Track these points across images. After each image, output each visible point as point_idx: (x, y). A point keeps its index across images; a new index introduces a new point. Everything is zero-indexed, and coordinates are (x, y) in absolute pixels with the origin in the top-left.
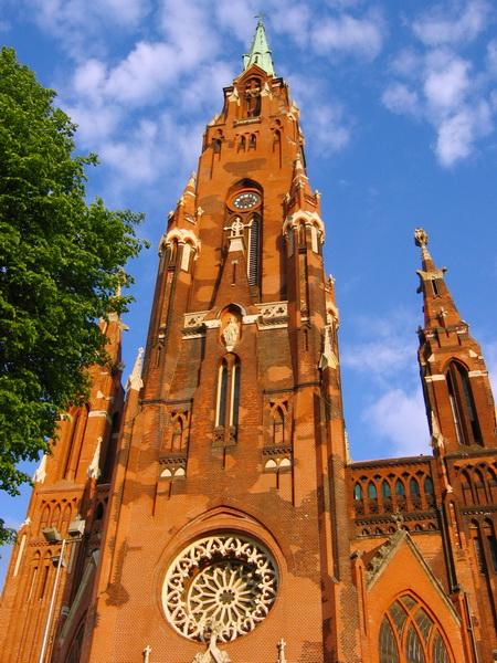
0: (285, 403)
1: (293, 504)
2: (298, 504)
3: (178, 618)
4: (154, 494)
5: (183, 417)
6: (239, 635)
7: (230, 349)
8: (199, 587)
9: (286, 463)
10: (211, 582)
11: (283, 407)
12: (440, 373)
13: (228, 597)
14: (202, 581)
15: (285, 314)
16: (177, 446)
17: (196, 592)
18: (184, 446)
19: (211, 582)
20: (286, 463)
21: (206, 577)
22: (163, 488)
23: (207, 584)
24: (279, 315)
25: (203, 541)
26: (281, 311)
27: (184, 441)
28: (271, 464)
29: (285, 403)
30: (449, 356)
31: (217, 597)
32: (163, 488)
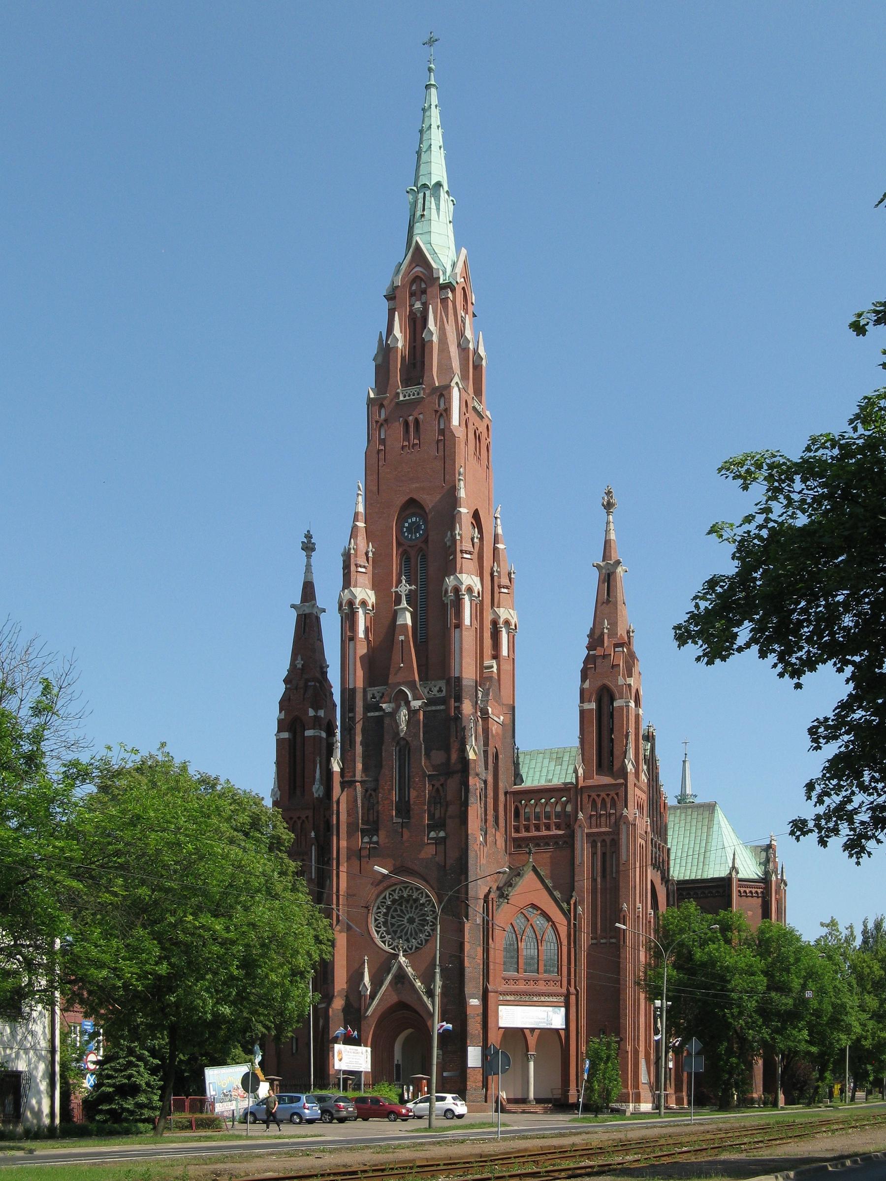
0: (442, 785)
1: (445, 866)
2: (447, 868)
3: (381, 937)
4: (360, 858)
5: (373, 793)
6: (417, 948)
7: (402, 735)
8: (395, 914)
9: (442, 834)
10: (402, 911)
11: (440, 788)
12: (590, 701)
13: (411, 921)
14: (396, 910)
15: (444, 694)
16: (371, 819)
17: (393, 917)
18: (375, 819)
19: (402, 911)
20: (442, 834)
21: (398, 908)
22: (365, 853)
23: (399, 912)
24: (438, 695)
25: (393, 888)
26: (440, 690)
27: (375, 814)
28: (432, 834)
29: (442, 785)
30: (600, 683)
31: (405, 920)
32: (365, 853)
